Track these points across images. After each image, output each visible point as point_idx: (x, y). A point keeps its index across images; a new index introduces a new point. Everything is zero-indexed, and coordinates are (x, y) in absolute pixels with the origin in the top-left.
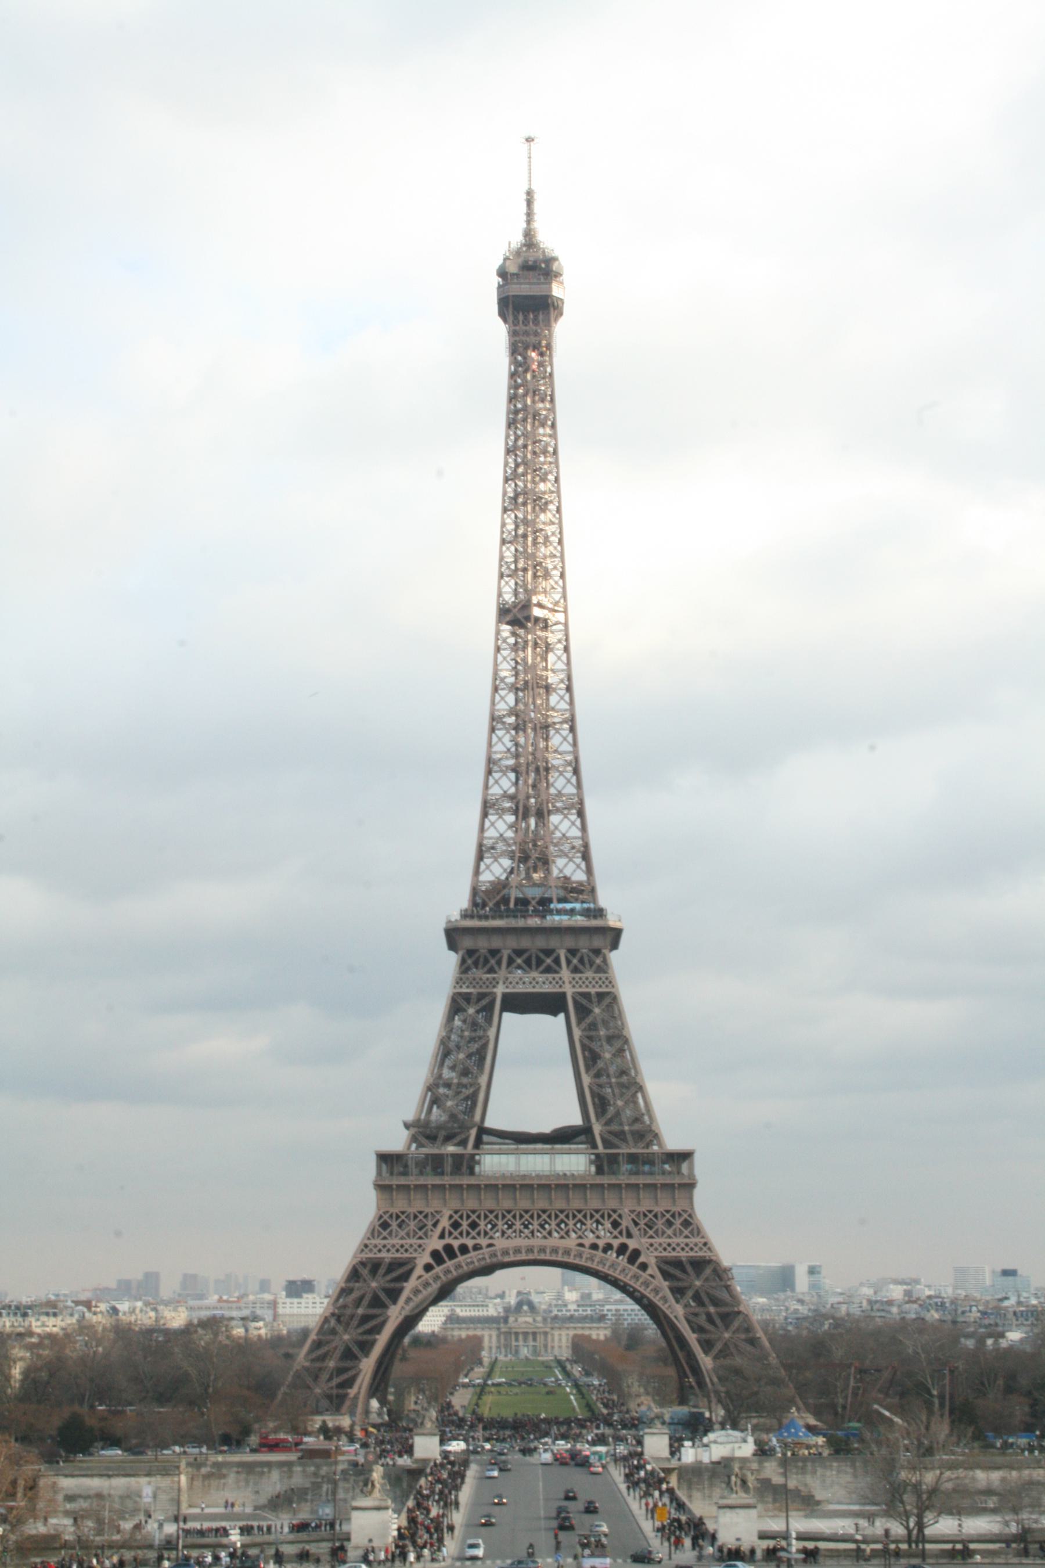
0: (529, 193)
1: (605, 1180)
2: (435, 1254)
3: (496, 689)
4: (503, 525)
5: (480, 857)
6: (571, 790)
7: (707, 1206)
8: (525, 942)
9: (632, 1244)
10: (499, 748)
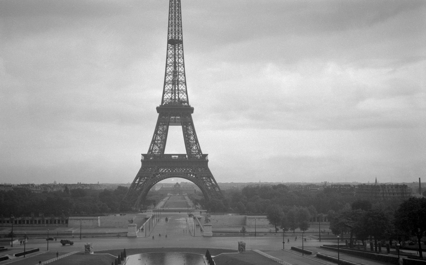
2: (154, 175)
4: (169, 22)
6: (183, 80)
7: (210, 165)
9: (195, 173)
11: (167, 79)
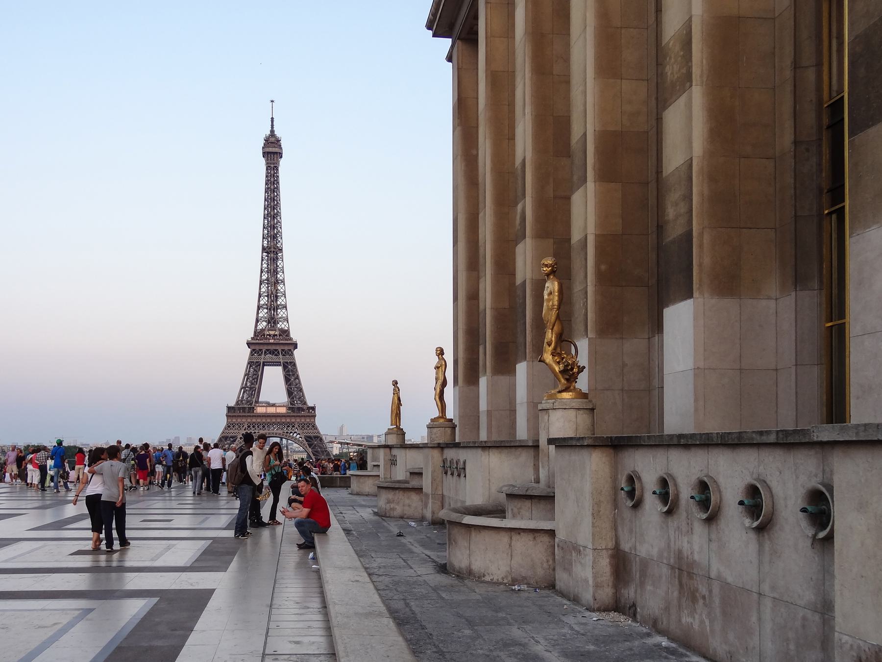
0: (272, 119)
1: (292, 414)
3: (262, 272)
5: (257, 321)
7: (318, 422)
8: (269, 347)
10: (263, 290)
11: (262, 302)
